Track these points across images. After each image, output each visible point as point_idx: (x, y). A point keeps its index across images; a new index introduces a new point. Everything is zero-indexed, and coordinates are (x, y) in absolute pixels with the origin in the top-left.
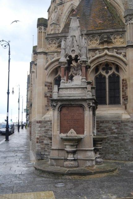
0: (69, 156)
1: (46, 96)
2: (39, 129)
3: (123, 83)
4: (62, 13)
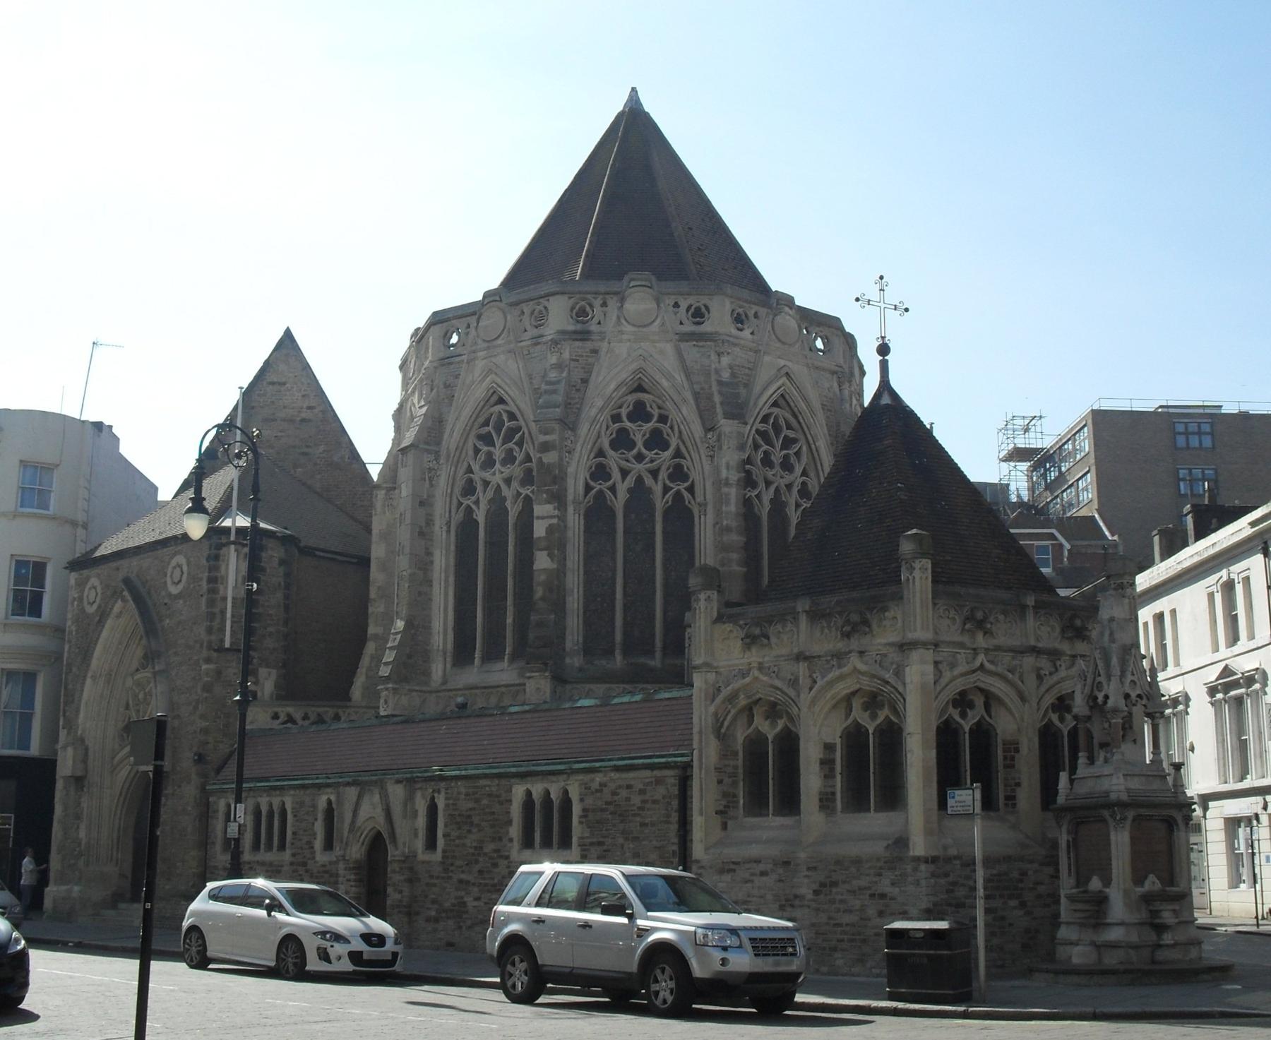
4: (585, 381)
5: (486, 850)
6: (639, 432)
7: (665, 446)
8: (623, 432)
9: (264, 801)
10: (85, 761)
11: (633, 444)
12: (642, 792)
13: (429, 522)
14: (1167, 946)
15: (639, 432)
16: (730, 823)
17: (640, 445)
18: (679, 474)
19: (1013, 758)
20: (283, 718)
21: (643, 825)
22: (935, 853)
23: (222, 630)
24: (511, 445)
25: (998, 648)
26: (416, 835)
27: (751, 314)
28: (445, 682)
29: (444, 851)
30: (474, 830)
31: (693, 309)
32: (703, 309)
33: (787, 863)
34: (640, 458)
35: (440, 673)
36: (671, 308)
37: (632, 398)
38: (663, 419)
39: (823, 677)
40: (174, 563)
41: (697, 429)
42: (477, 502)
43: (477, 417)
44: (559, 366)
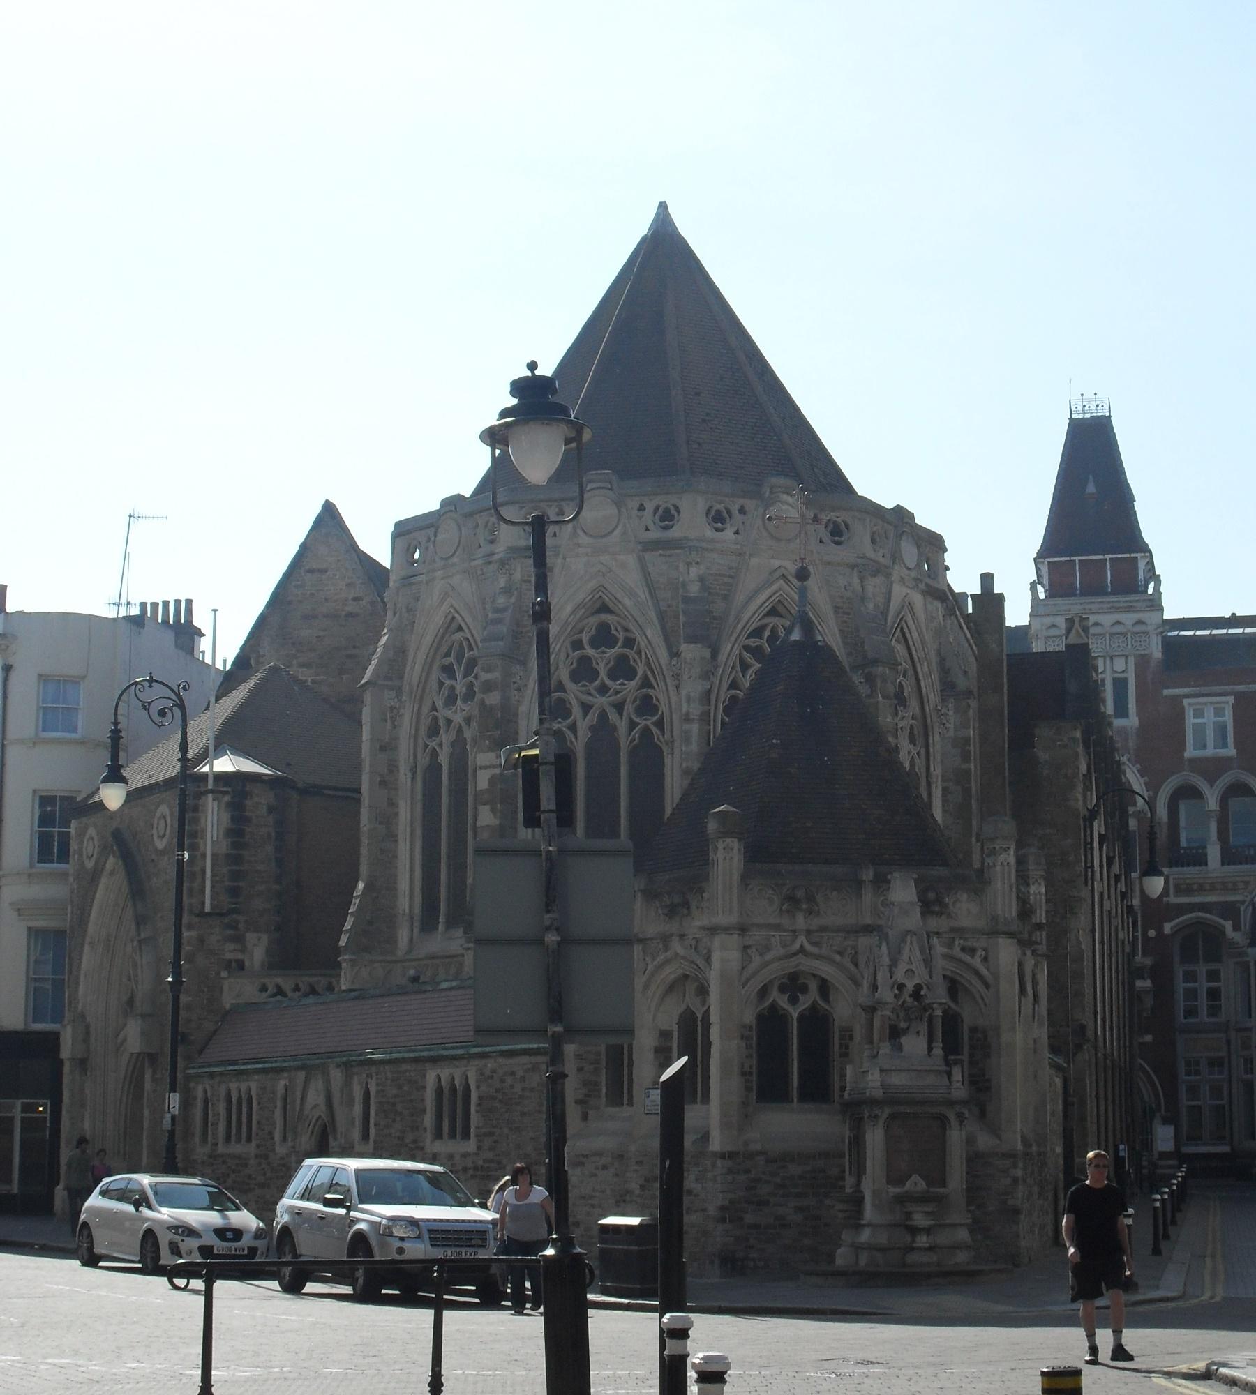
0: (918, 1238)
1: (743, 1074)
2: (730, 1178)
3: (971, 1038)
5: (407, 1141)
6: (602, 660)
7: (630, 674)
8: (585, 661)
9: (233, 1086)
10: (86, 1040)
11: (596, 674)
12: (523, 1079)
13: (393, 767)
14: (919, 1249)
15: (602, 660)
16: (591, 1113)
17: (603, 675)
18: (647, 706)
19: (847, 1047)
20: (271, 990)
21: (523, 1114)
22: (729, 1148)
23: (203, 891)
24: (470, 678)
25: (823, 929)
26: (353, 1123)
27: (735, 509)
28: (410, 951)
29: (375, 1142)
30: (398, 1119)
31: (660, 512)
32: (673, 512)
33: (622, 1156)
34: (603, 690)
35: (406, 940)
36: (635, 512)
37: (594, 621)
38: (629, 643)
39: (654, 960)
40: (158, 814)
41: (663, 654)
42: (441, 745)
43: (438, 649)
44: (507, 591)
